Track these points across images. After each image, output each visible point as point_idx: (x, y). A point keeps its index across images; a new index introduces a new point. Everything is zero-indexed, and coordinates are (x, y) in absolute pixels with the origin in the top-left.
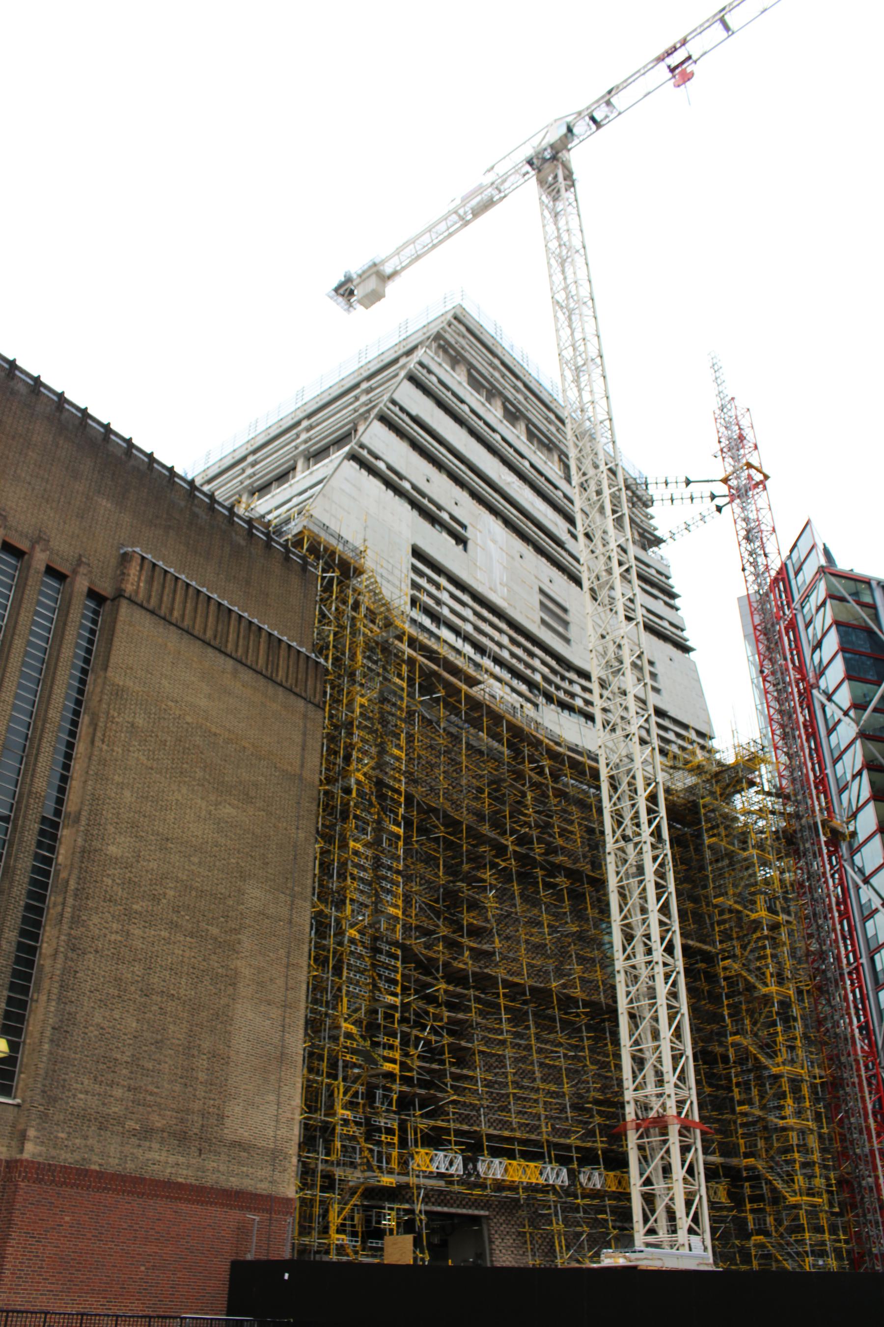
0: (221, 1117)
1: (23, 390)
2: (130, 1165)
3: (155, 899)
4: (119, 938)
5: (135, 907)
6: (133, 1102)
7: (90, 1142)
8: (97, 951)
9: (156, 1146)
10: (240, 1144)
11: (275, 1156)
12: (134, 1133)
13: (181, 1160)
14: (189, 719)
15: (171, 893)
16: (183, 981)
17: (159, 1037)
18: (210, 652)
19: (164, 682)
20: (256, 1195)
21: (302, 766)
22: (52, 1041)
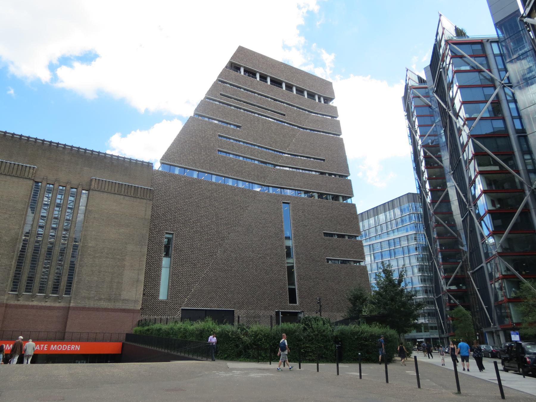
0: (120, 295)
1: (61, 149)
2: (96, 306)
3: (102, 253)
4: (92, 262)
7: (86, 302)
10: (125, 300)
11: (136, 301)
12: (97, 300)
13: (109, 304)
14: (110, 212)
15: (106, 251)
18: (116, 196)
22: (76, 284)
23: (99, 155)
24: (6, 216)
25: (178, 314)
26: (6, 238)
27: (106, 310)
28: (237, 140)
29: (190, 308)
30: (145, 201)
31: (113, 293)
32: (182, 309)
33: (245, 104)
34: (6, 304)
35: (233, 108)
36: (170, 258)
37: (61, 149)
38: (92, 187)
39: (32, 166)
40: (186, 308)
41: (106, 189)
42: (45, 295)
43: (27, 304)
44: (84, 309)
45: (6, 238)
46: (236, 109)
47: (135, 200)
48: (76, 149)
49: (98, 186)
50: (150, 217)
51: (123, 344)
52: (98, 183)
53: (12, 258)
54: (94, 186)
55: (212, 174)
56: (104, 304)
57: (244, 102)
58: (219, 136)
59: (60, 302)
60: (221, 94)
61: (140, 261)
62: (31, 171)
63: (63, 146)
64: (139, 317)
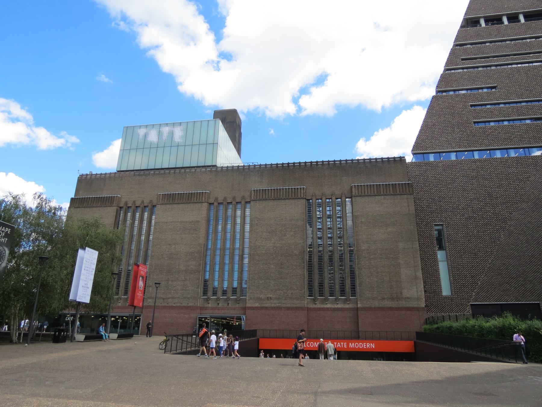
0: (401, 293)
1: (320, 166)
4: (369, 264)
5: (371, 257)
6: (379, 294)
7: (371, 302)
8: (364, 268)
9: (386, 301)
11: (418, 299)
12: (381, 299)
15: (379, 252)
16: (386, 268)
17: (382, 280)
18: (377, 197)
19: (367, 209)
20: (414, 307)
21: (409, 211)
22: (359, 286)
23: (352, 163)
24: (292, 233)
25: (468, 310)
26: (296, 251)
27: (391, 309)
28: (495, 104)
29: (480, 303)
30: (405, 196)
31: (394, 292)
32: (471, 305)
33: (495, 59)
34: (308, 308)
35: (480, 69)
36: (445, 251)
37: (320, 166)
38: (354, 194)
39: (302, 187)
40: (475, 303)
41: (366, 193)
42: (335, 298)
43: (323, 307)
44: (370, 309)
45: (296, 251)
46: (485, 69)
47: (395, 197)
48: (332, 163)
49: (358, 192)
50: (414, 212)
51: (415, 342)
52: (358, 188)
53: (304, 268)
54: (355, 192)
55: (473, 151)
56: (388, 304)
57: (494, 57)
58: (472, 106)
59: (349, 304)
60: (463, 60)
61: (414, 258)
62: (302, 191)
63: (321, 163)
64: (426, 315)
